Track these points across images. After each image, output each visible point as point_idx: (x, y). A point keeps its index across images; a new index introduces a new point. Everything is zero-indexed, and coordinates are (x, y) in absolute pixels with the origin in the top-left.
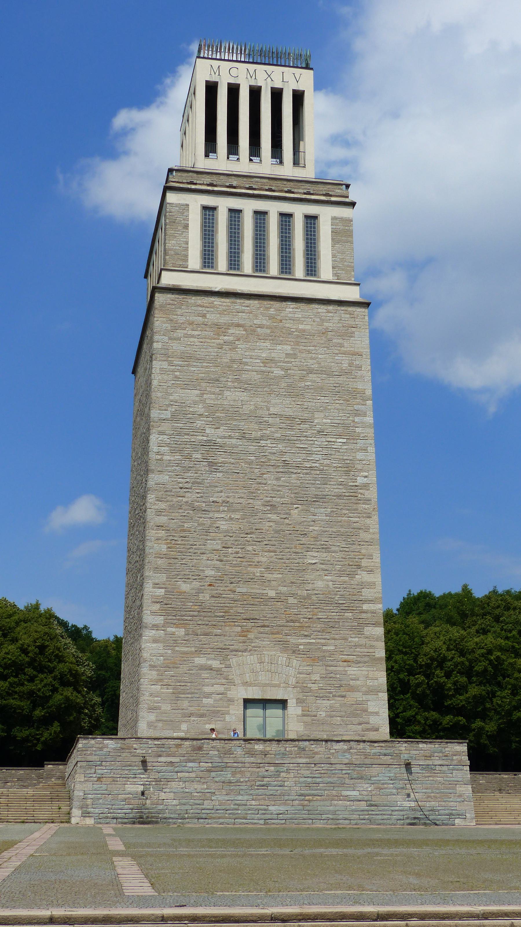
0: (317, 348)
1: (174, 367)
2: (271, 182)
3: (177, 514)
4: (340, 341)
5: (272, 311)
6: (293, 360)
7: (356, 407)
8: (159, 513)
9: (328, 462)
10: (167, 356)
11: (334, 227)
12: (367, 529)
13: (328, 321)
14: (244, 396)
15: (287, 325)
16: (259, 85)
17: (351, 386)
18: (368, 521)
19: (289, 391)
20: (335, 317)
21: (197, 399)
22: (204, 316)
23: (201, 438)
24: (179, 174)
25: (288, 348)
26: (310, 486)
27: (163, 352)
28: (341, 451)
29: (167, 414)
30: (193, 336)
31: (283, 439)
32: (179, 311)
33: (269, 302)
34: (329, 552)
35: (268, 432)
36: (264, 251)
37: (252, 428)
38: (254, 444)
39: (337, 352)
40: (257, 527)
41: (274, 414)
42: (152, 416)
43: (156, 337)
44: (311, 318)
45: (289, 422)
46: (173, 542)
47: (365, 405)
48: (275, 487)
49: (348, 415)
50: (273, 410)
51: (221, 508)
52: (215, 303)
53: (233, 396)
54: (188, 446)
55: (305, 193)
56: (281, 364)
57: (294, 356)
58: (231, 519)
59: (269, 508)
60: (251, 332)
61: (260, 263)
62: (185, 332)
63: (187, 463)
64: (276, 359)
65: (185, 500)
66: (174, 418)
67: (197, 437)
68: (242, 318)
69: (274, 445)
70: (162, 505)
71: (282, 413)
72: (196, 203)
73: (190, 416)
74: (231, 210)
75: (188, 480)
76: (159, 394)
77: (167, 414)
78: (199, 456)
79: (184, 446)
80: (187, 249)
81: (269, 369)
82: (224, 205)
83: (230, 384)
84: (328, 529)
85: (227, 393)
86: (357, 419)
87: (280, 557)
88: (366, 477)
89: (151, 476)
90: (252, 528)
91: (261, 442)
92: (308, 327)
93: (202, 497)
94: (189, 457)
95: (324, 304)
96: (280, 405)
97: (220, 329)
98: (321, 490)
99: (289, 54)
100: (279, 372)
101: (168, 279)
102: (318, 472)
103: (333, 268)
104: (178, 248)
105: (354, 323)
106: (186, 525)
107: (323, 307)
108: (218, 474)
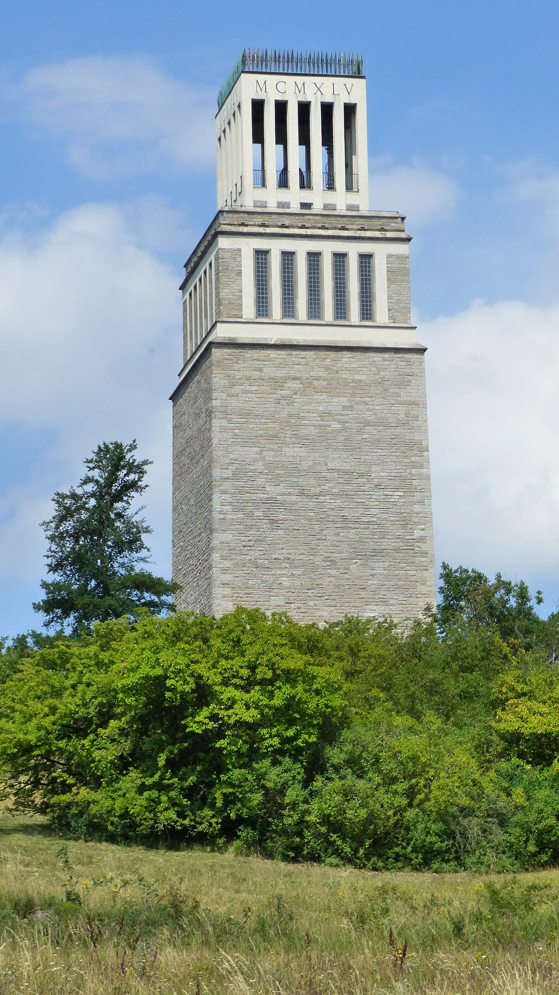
0: (374, 399)
1: (233, 425)
2: (324, 219)
3: (242, 572)
4: (397, 390)
5: (328, 362)
6: (350, 413)
7: (413, 459)
8: (224, 571)
9: (386, 516)
11: (390, 265)
12: (424, 582)
13: (385, 370)
14: (302, 452)
15: (344, 376)
16: (308, 100)
17: (408, 438)
18: (425, 574)
19: (346, 444)
20: (391, 365)
21: (257, 456)
22: (261, 370)
23: (262, 496)
24: (230, 215)
25: (344, 400)
26: (369, 540)
27: (221, 409)
28: (398, 504)
29: (228, 473)
30: (251, 392)
31: (342, 494)
32: (236, 367)
33: (325, 353)
34: (387, 605)
35: (326, 488)
36: (318, 295)
37: (310, 483)
38: (313, 500)
39: (394, 402)
40: (318, 583)
41: (332, 469)
42: (214, 475)
43: (215, 395)
44: (367, 367)
45: (346, 476)
46: (239, 599)
47: (422, 456)
48: (334, 543)
49: (405, 468)
50: (330, 466)
51: (283, 565)
52: (271, 356)
53: (291, 452)
54: (250, 504)
55: (359, 230)
56: (338, 417)
57: (351, 408)
58: (293, 575)
59: (329, 563)
60: (308, 385)
61: (315, 308)
62: (243, 387)
63: (249, 522)
64: (333, 412)
65: (248, 557)
66: (235, 476)
67: (258, 495)
68: (297, 371)
69: (333, 501)
70: (227, 564)
71: (340, 468)
72: (248, 247)
73: (250, 474)
74: (284, 253)
75: (250, 538)
76: (220, 453)
77: (228, 473)
78: (261, 514)
79: (245, 504)
80: (241, 298)
81: (326, 423)
82: (276, 247)
83: (288, 440)
84: (385, 583)
85: (286, 450)
86: (414, 471)
87: (340, 611)
88: (423, 530)
89: (215, 535)
90: (313, 584)
91: (320, 498)
92: (364, 377)
93: (264, 554)
94: (251, 515)
95: (380, 352)
96: (338, 460)
97: (277, 383)
98: (379, 544)
99: (339, 61)
100: (336, 426)
101: (223, 332)
102: (376, 527)
103: (389, 310)
104: (232, 297)
105: (410, 371)
106: (250, 583)
107: (379, 355)
108: (279, 531)
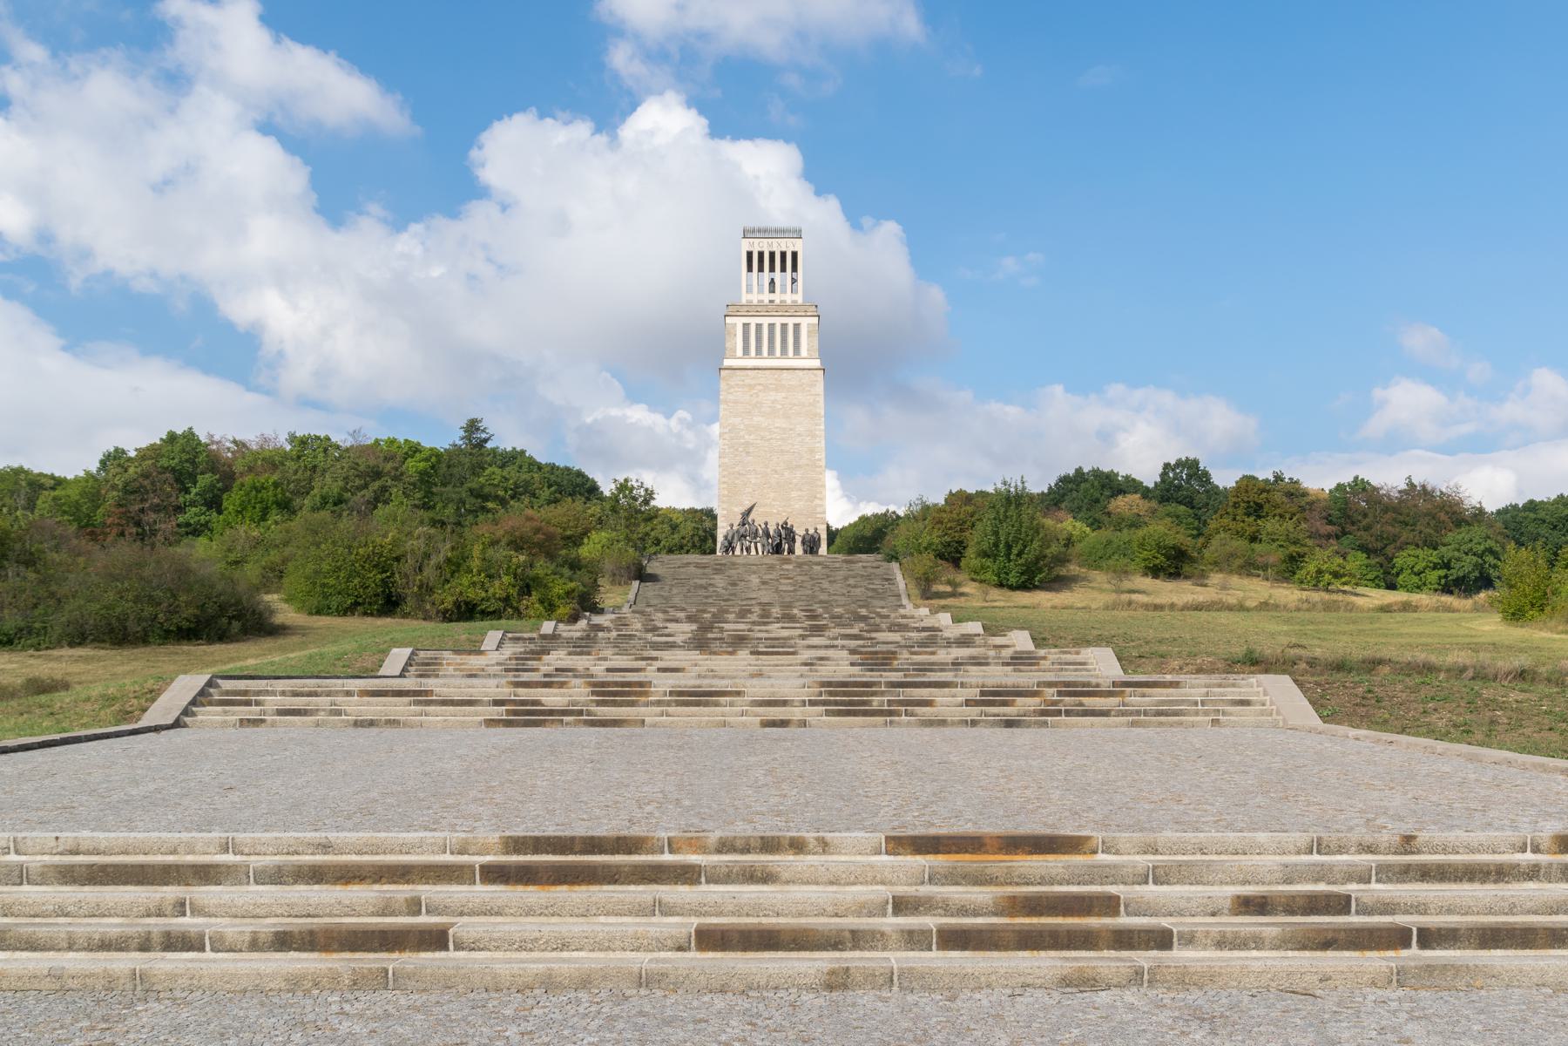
10: (726, 402)
82: (753, 321)
97: (751, 387)
101: (727, 363)
